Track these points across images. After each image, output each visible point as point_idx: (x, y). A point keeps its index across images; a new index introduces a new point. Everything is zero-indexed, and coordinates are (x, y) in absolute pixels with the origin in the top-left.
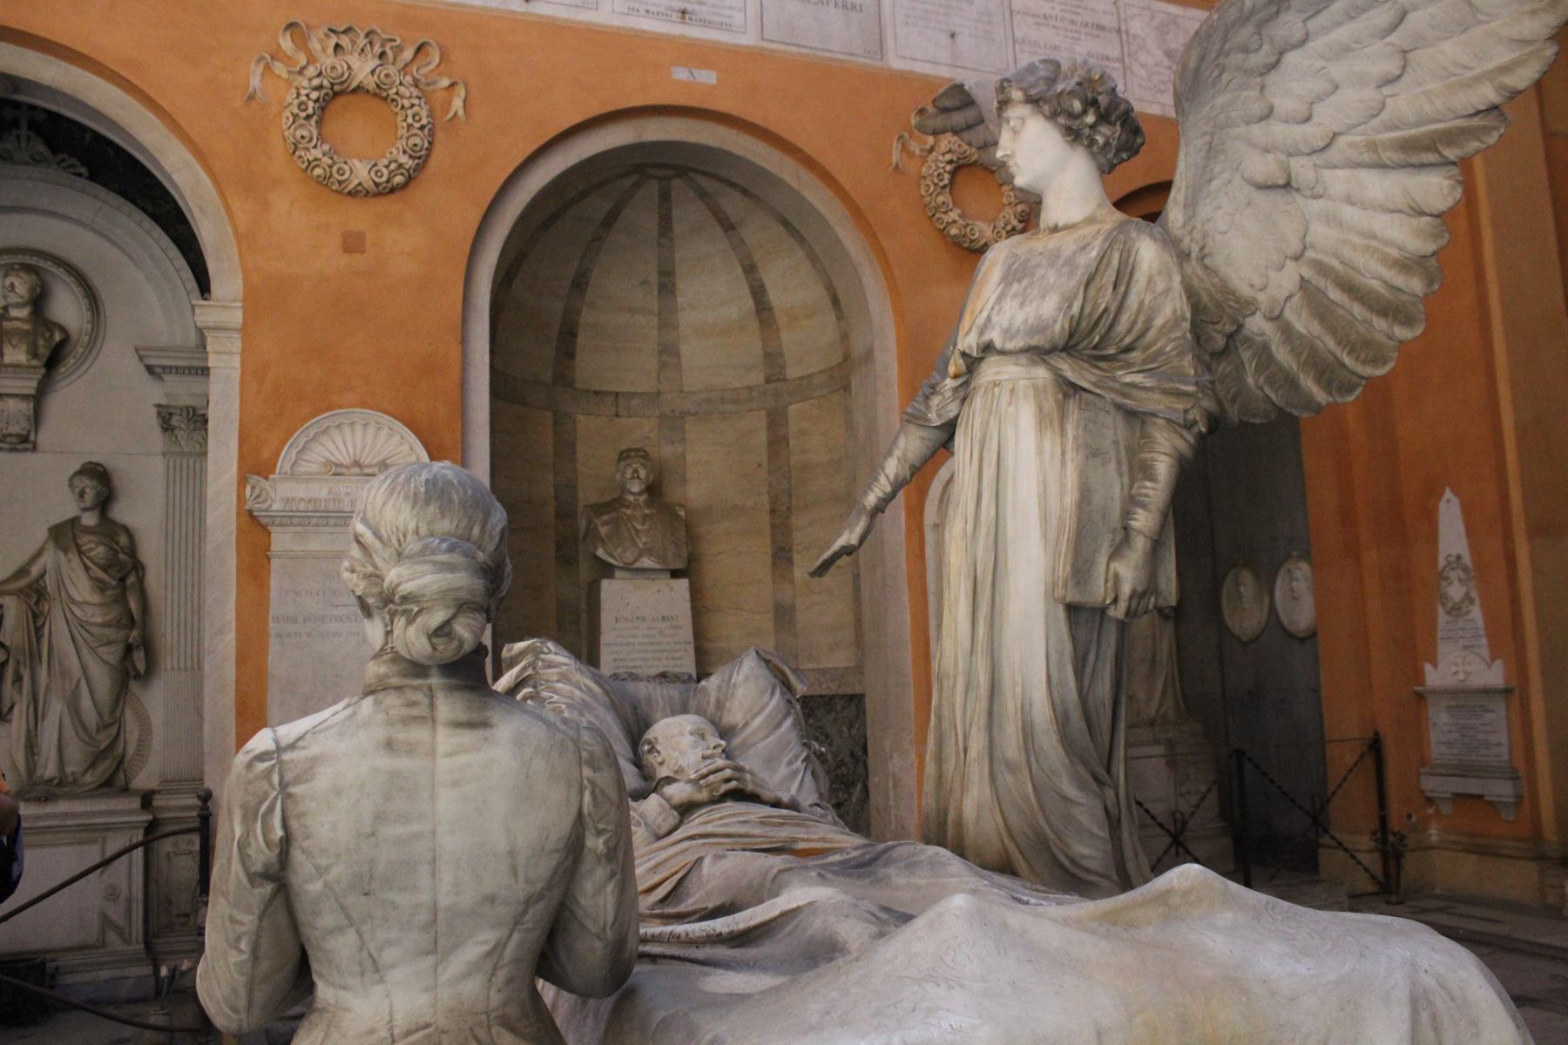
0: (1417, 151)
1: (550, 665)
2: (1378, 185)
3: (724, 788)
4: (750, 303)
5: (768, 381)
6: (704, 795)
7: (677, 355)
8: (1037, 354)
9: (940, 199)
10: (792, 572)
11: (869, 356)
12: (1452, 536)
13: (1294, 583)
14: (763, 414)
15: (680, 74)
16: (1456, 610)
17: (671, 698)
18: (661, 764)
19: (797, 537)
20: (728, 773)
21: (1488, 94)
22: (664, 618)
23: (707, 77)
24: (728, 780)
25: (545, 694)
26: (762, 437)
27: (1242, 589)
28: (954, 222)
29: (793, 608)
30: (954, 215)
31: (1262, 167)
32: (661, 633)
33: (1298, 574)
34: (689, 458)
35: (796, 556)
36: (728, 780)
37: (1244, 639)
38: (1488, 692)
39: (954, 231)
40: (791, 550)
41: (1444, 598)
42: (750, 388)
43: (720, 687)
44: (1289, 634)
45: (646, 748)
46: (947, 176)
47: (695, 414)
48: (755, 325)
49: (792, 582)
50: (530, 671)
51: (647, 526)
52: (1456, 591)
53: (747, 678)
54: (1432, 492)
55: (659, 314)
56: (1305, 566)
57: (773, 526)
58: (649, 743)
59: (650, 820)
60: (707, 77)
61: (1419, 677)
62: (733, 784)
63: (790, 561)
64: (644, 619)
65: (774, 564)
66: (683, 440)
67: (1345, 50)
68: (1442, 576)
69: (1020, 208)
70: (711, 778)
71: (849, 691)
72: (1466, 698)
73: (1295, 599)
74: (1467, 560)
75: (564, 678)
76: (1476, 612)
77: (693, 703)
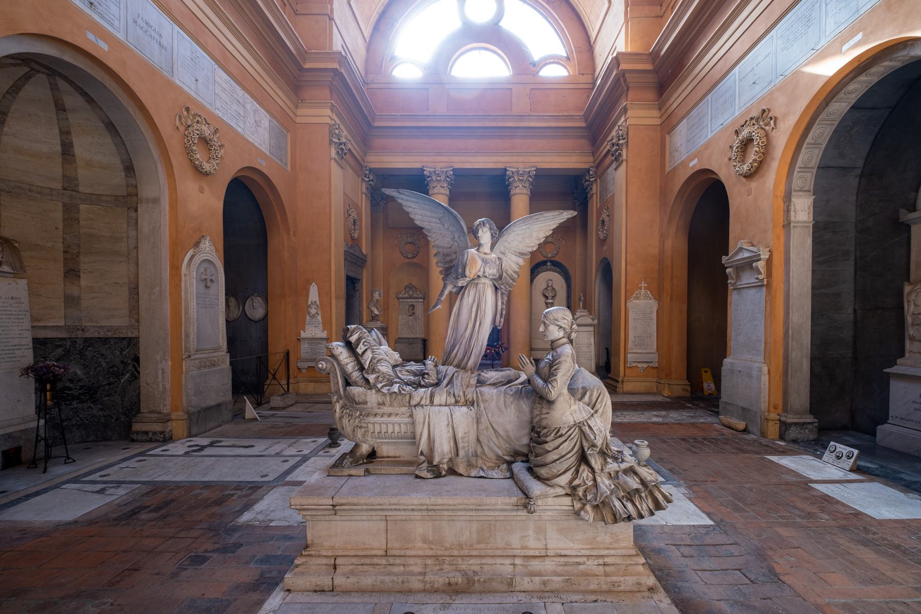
0: (522, 254)
2: (514, 258)
8: (492, 280)
11: (156, 201)
12: (314, 294)
15: (91, 36)
16: (313, 316)
21: (530, 250)
22: (12, 298)
23: (105, 46)
29: (79, 298)
31: (502, 249)
35: (82, 275)
38: (322, 339)
40: (79, 271)
41: (309, 313)
42: (52, 190)
48: (60, 160)
49: (79, 286)
52: (313, 311)
54: (308, 283)
57: (65, 259)
60: (105, 46)
61: (300, 334)
65: (65, 276)
67: (518, 235)
68: (309, 306)
71: (121, 336)
72: (313, 340)
74: (318, 303)
76: (319, 318)
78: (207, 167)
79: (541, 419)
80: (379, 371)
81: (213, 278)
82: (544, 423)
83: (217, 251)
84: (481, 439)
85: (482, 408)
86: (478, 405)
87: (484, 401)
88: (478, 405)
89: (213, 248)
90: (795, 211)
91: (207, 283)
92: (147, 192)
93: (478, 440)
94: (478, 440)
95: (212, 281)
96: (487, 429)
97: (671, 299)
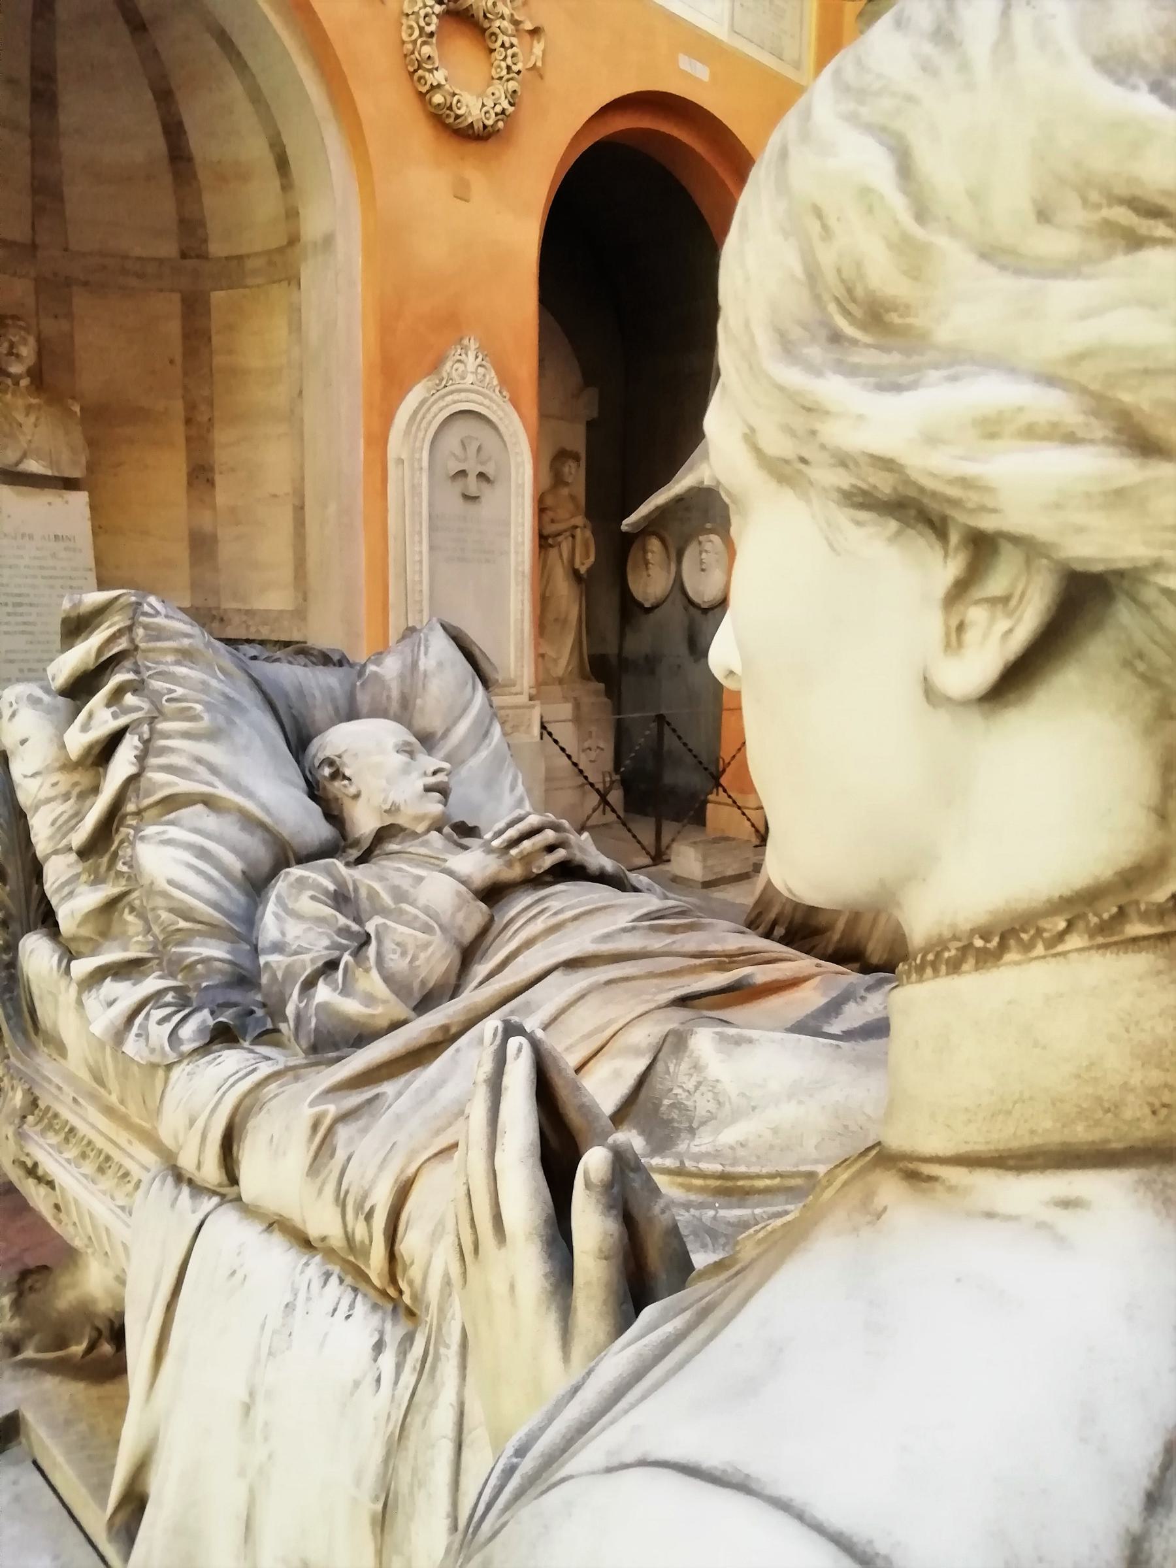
1: (158, 634)
3: (549, 860)
4: (160, 145)
5: (184, 255)
6: (516, 872)
7: (59, 197)
9: (426, 50)
10: (214, 497)
11: (328, 241)
13: (704, 555)
14: (176, 297)
17: (331, 689)
18: (357, 796)
19: (221, 456)
20: (549, 835)
22: (56, 537)
24: (550, 848)
25: (157, 684)
26: (173, 328)
27: (650, 556)
28: (439, 86)
30: (439, 77)
32: (54, 555)
33: (708, 546)
34: (79, 339)
35: (219, 479)
36: (550, 848)
37: (647, 605)
39: (438, 98)
40: (212, 469)
42: (161, 261)
43: (402, 677)
44: (691, 602)
45: (327, 771)
46: (435, 20)
47: (86, 284)
48: (167, 179)
49: (213, 507)
50: (123, 644)
51: (32, 419)
53: (440, 664)
55: (32, 135)
56: (714, 538)
57: (189, 440)
58: (330, 762)
59: (445, 919)
62: (561, 854)
63: (211, 483)
64: (31, 537)
65: (190, 484)
66: (70, 316)
69: (512, 85)
70: (527, 844)
73: (703, 570)
75: (186, 656)
77: (363, 699)
78: (473, 108)
80: (134, 876)
81: (489, 470)
83: (506, 380)
89: (492, 377)
91: (473, 483)
92: (313, 225)
95: (481, 475)
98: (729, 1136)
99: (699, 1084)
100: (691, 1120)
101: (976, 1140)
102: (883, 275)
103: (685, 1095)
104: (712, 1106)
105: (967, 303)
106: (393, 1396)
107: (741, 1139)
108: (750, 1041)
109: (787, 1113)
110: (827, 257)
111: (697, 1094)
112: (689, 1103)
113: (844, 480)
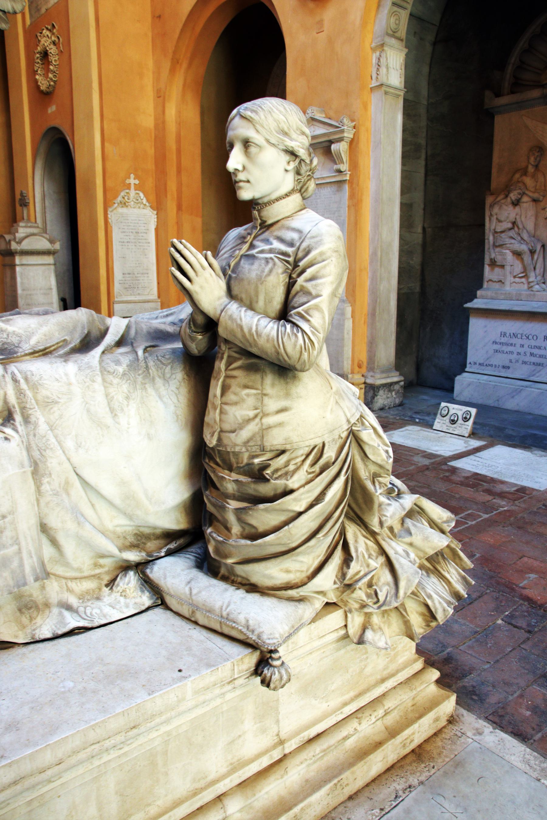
79: (264, 431)
82: (275, 440)
84: (53, 521)
85: (43, 427)
86: (26, 420)
87: (48, 404)
88: (26, 420)
90: (387, 68)
93: (44, 528)
94: (44, 528)
96: (66, 487)
97: (179, 207)
98: (33, 341)
99: (8, 335)
100: (14, 345)
101: (294, 212)
102: (286, 129)
103: (5, 340)
104: (18, 338)
105: (294, 135)
106: (20, 436)
107: (37, 341)
108: (11, 319)
109: (45, 329)
110: (280, 125)
111: (10, 338)
112: (9, 341)
113: (285, 148)
